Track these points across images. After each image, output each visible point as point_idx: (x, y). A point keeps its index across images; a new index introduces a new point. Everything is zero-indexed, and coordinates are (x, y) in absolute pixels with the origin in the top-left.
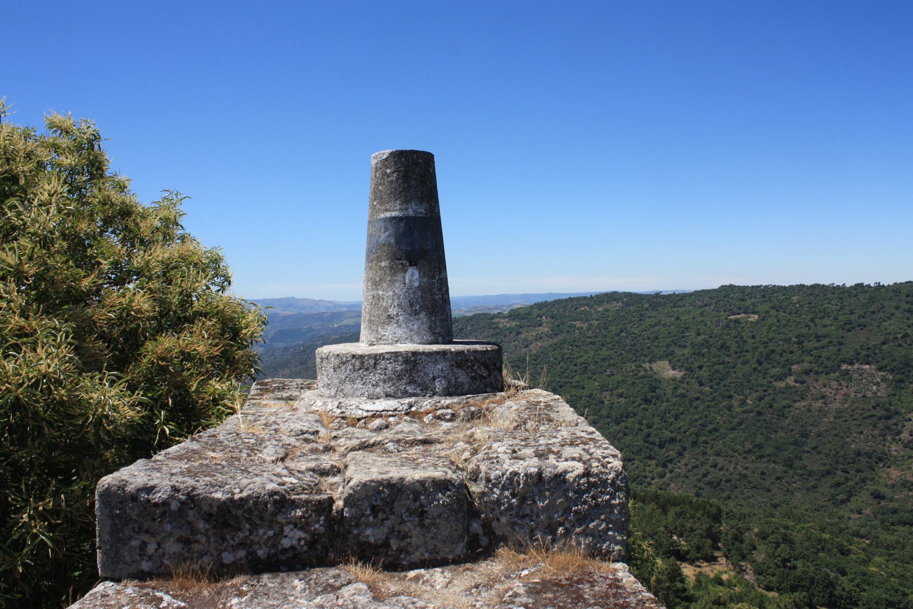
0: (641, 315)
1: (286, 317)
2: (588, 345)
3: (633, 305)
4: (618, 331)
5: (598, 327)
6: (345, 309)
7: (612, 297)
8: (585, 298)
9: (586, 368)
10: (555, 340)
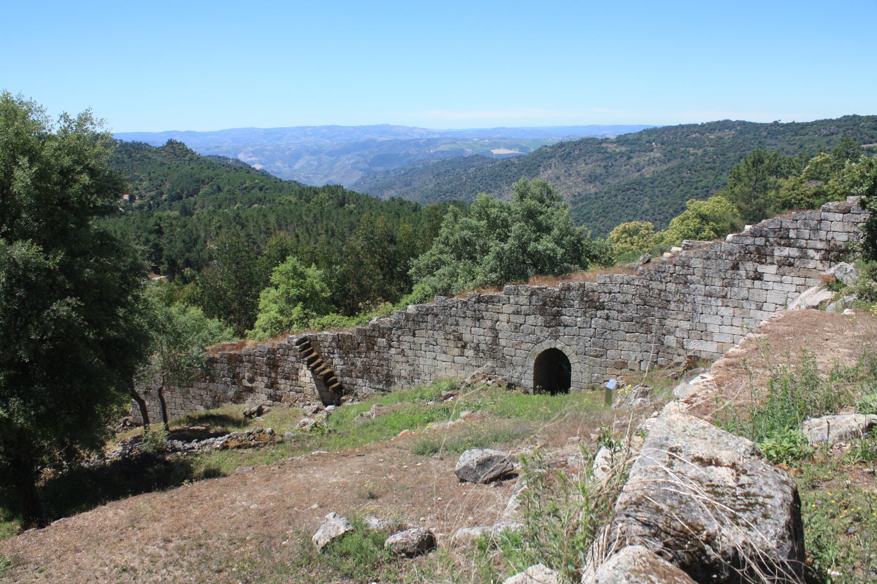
0: (760, 143)
1: (383, 143)
2: (707, 169)
3: (748, 133)
4: (737, 157)
5: (715, 153)
6: (438, 136)
7: (725, 125)
8: (695, 126)
9: (708, 191)
10: (670, 165)
